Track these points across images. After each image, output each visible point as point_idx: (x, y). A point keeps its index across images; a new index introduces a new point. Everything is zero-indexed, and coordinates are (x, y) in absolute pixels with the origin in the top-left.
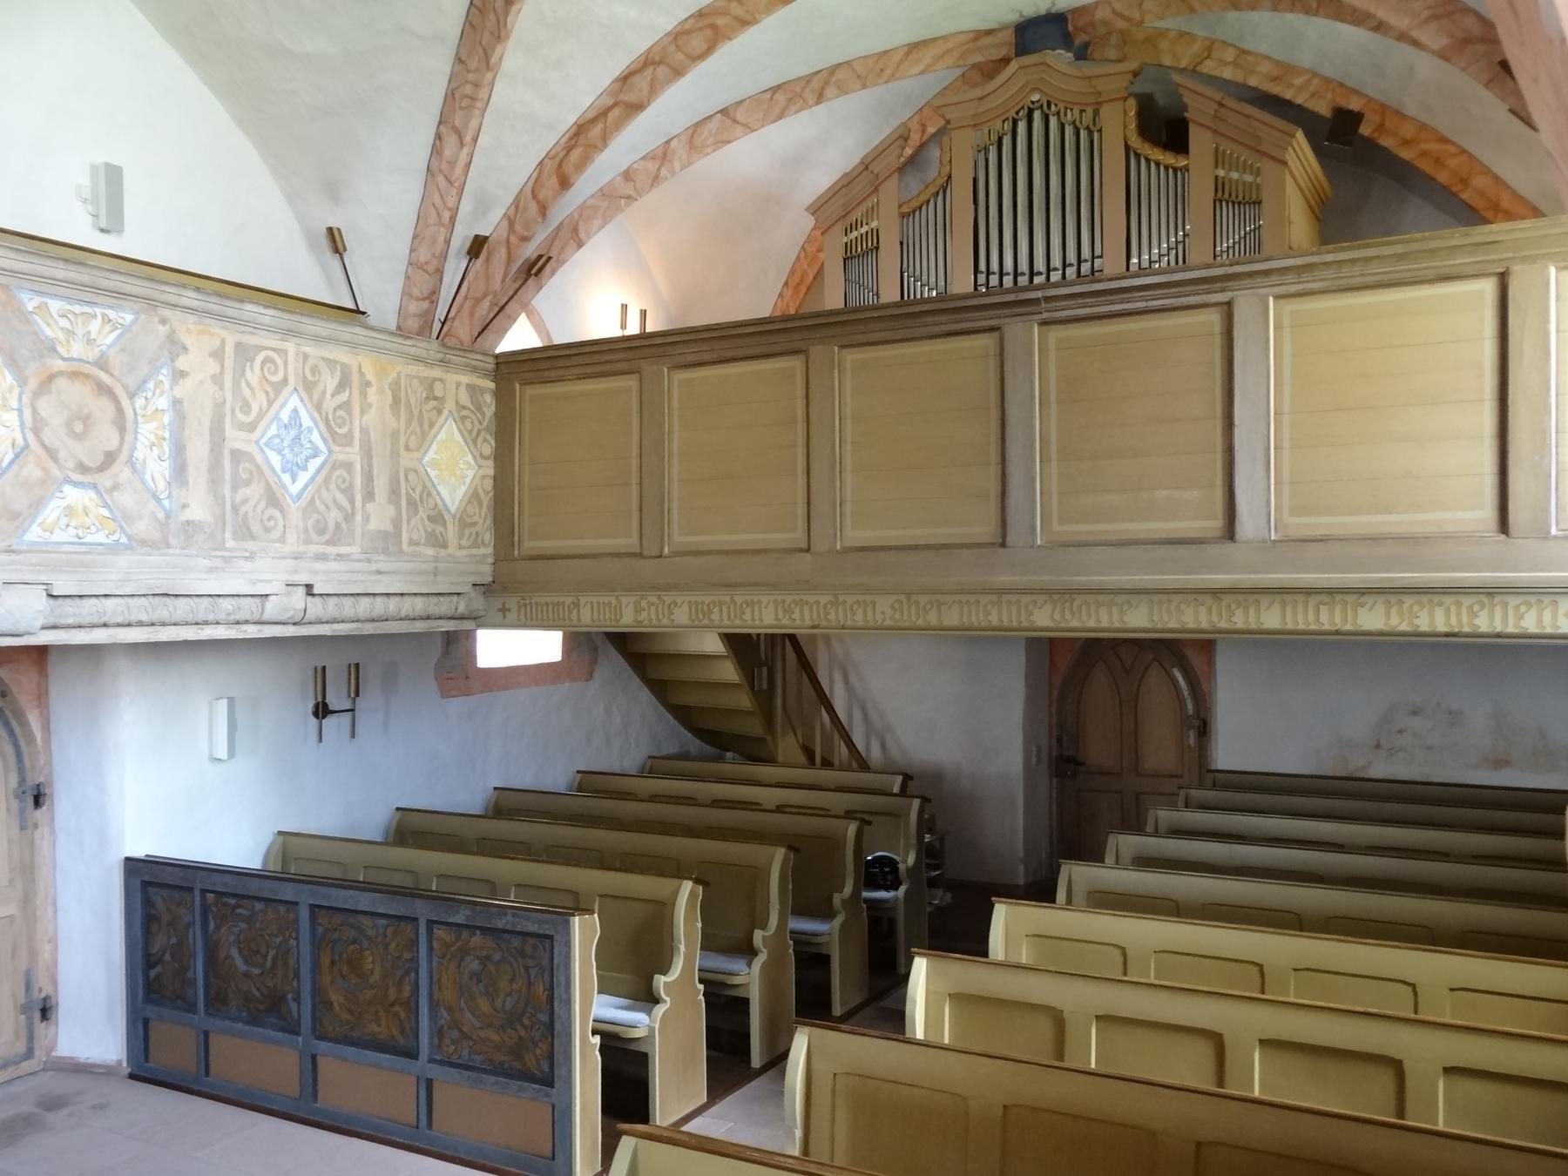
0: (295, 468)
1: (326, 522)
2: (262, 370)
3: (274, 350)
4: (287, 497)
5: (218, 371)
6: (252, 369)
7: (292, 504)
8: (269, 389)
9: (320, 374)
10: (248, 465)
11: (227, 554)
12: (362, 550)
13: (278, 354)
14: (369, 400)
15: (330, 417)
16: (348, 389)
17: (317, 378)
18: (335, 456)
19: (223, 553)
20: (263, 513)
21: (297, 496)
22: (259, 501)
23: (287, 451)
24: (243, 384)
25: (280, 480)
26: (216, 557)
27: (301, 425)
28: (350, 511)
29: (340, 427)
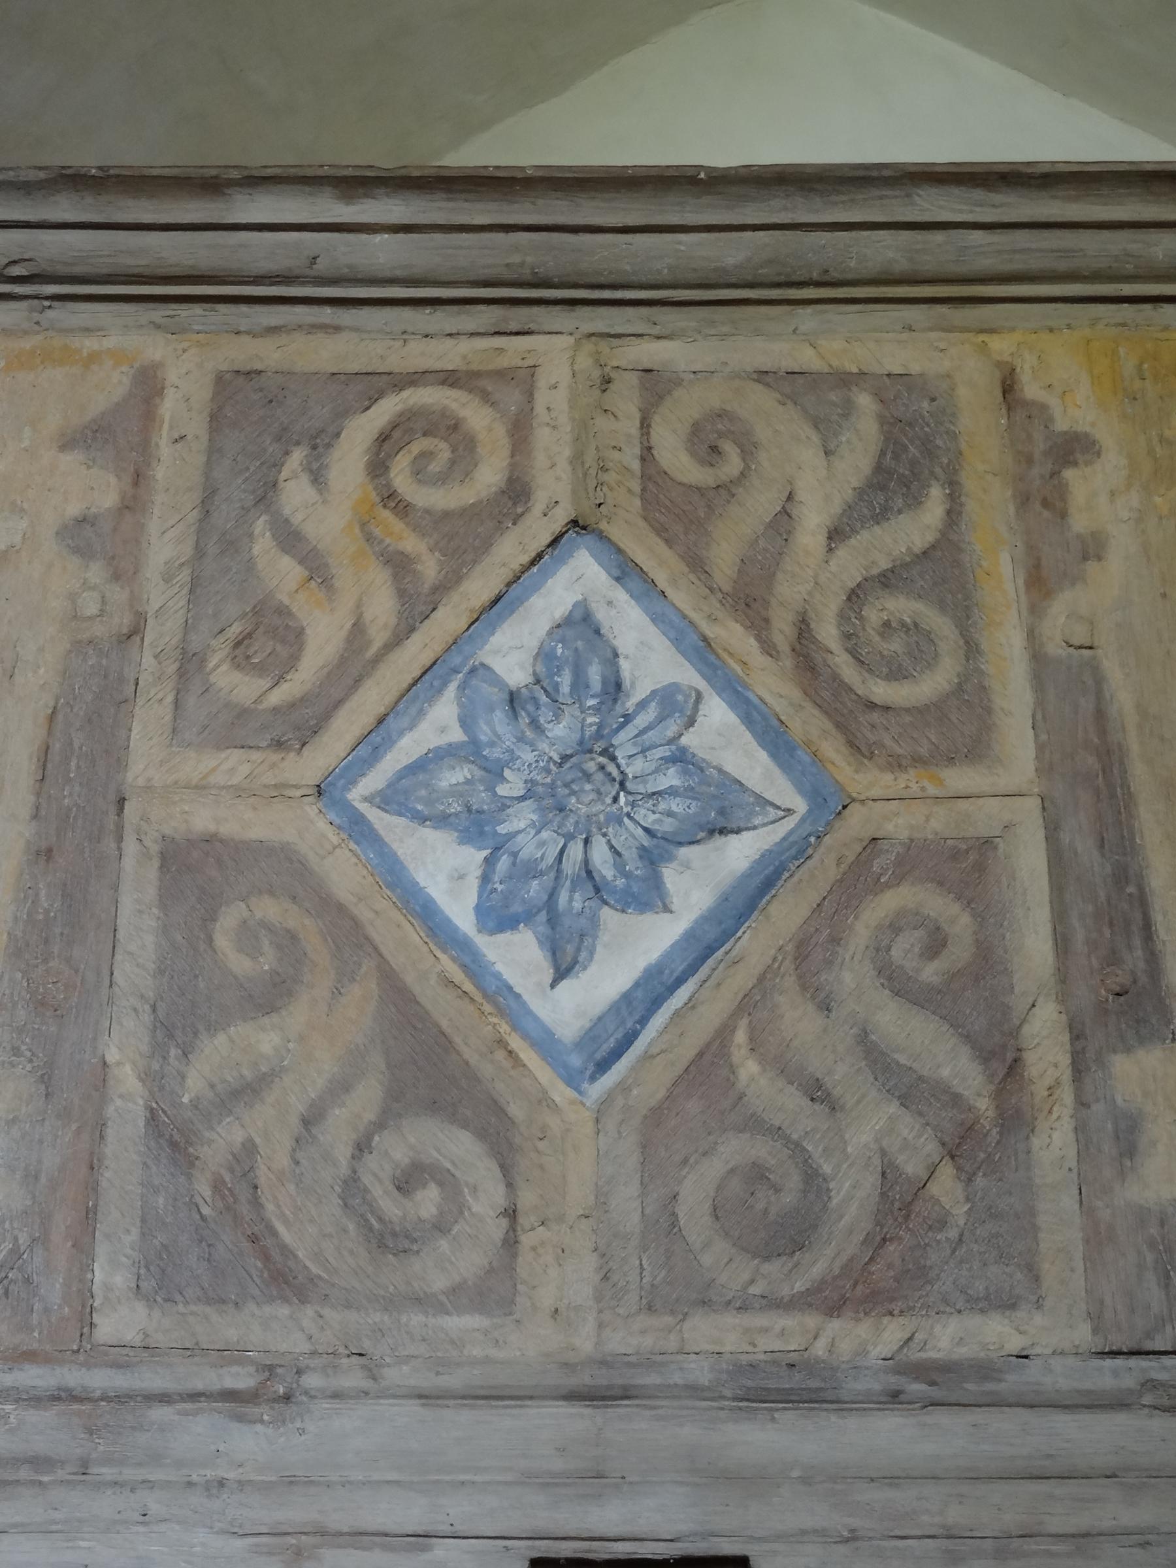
0: (572, 901)
1: (813, 1179)
2: (378, 467)
3: (450, 379)
4: (528, 1056)
5: (107, 498)
6: (317, 478)
7: (561, 1093)
8: (411, 544)
9: (748, 449)
10: (269, 909)
11: (100, 1380)
12: (1096, 1319)
13: (486, 398)
14: (1079, 523)
15: (828, 632)
16: (936, 492)
17: (733, 464)
18: (856, 823)
19: (72, 1377)
20: (362, 1147)
21: (591, 1036)
22: (341, 1087)
23: (521, 819)
24: (263, 545)
25: (474, 965)
26: (37, 1400)
27: (615, 688)
28: (984, 1105)
29: (896, 674)
